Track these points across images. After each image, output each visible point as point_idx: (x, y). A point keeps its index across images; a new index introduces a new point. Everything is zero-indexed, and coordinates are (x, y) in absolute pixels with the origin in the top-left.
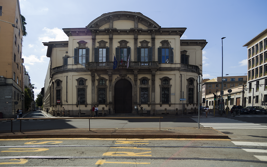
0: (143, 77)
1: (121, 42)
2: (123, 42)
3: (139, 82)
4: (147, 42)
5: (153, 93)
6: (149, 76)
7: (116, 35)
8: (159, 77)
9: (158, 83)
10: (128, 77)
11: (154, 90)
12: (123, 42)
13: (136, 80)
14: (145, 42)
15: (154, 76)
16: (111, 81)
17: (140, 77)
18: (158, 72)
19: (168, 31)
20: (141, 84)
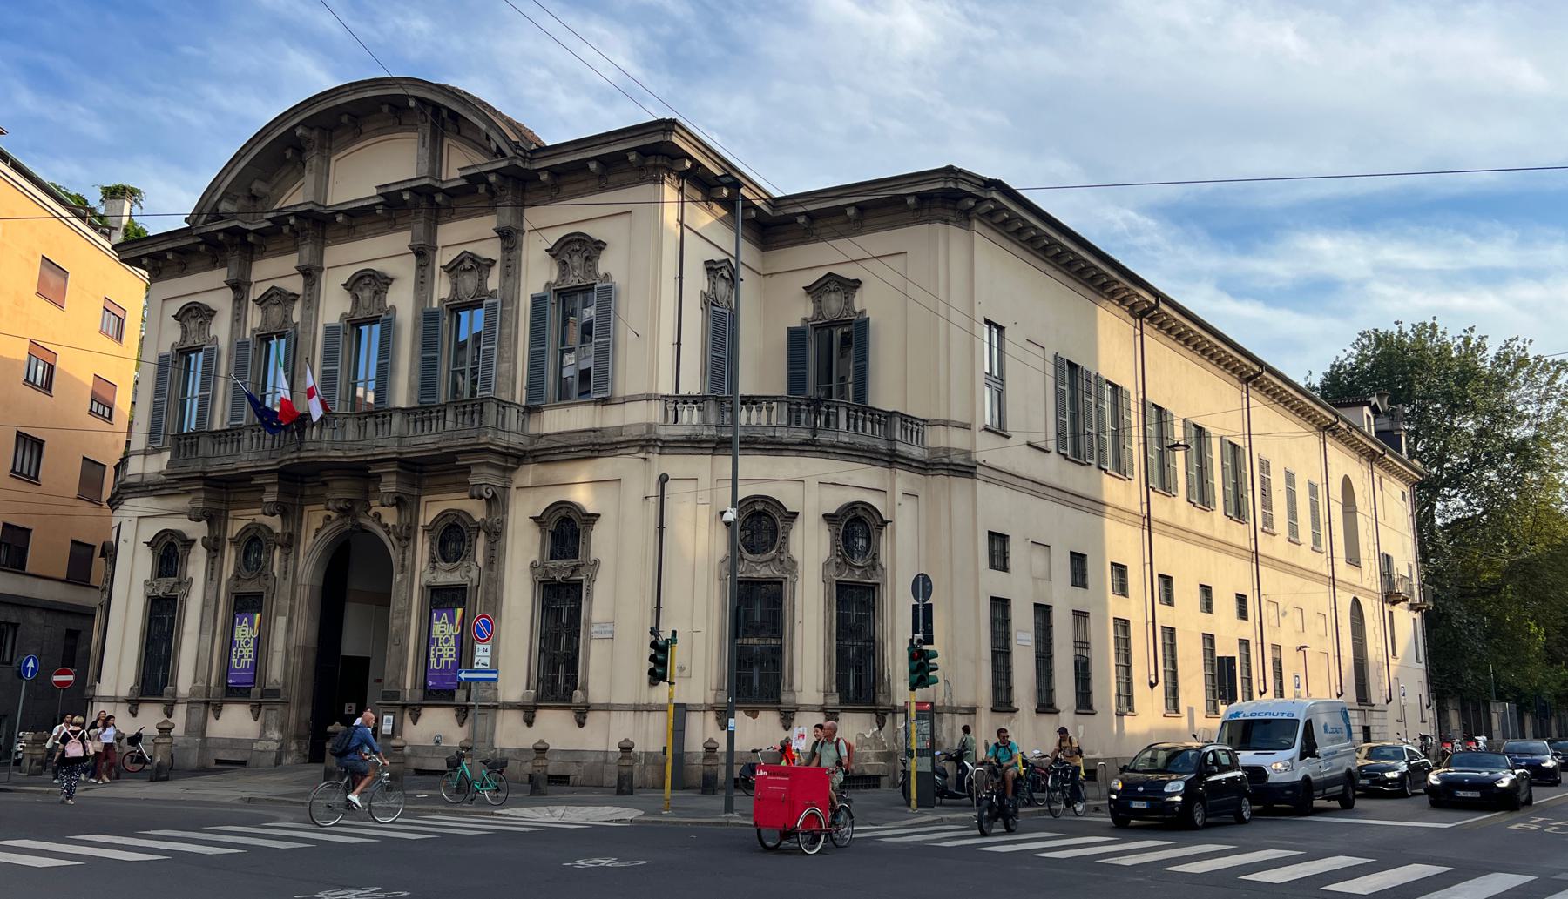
1: (353, 285)
3: (423, 546)
9: (523, 548)
17: (430, 511)
18: (528, 474)
19: (582, 166)
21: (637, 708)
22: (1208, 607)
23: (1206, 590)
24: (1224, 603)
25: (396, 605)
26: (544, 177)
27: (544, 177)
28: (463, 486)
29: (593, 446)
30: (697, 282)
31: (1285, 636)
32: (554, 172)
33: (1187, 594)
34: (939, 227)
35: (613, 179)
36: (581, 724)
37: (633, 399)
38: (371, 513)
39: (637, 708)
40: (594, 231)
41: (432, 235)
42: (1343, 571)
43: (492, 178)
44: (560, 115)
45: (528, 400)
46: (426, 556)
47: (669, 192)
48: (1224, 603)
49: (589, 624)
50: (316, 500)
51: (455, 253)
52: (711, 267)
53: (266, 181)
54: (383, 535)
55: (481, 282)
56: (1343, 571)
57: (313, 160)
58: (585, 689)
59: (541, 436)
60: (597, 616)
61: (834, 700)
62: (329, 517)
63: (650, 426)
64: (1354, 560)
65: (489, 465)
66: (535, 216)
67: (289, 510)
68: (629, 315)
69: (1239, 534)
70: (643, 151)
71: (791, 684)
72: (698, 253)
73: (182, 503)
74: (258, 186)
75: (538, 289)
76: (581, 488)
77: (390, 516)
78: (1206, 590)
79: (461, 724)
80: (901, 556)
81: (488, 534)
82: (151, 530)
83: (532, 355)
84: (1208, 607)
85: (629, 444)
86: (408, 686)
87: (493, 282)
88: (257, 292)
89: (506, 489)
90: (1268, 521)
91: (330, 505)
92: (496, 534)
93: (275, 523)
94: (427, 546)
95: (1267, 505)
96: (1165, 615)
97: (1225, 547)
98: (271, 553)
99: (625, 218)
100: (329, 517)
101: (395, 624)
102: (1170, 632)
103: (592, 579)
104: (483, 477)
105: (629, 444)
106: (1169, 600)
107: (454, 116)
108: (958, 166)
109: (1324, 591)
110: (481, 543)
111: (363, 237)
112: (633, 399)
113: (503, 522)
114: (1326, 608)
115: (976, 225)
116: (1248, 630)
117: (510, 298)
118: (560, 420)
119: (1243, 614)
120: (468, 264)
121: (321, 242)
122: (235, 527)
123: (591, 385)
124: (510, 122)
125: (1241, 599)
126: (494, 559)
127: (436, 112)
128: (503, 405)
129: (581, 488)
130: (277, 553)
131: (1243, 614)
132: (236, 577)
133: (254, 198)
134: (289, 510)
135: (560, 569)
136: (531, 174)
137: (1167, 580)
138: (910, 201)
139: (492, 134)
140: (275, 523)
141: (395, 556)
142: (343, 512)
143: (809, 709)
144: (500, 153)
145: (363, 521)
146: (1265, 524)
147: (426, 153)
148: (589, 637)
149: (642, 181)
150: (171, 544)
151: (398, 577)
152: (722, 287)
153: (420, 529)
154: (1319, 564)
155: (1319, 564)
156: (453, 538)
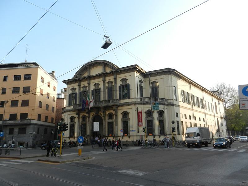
0: (109, 113)
1: (95, 85)
2: (97, 85)
3: (107, 117)
4: (112, 82)
5: (116, 127)
6: (114, 113)
7: (92, 80)
8: (120, 111)
9: (120, 117)
10: (100, 114)
11: (117, 125)
12: (97, 85)
13: (104, 116)
14: (110, 82)
15: (116, 112)
16: (89, 117)
17: (107, 112)
18: (120, 108)
19: (125, 70)
20: (108, 119)
22: (200, 120)
23: (200, 118)
24: (202, 120)
25: (104, 124)
26: (120, 71)
27: (120, 71)
28: (112, 109)
30: (139, 83)
31: (209, 123)
34: (167, 75)
35: (128, 71)
37: (133, 98)
41: (105, 79)
42: (216, 115)
43: (113, 72)
44: (121, 64)
47: (135, 73)
48: (202, 120)
51: (108, 81)
53: (82, 72)
54: (101, 116)
55: (112, 84)
56: (216, 115)
57: (88, 70)
59: (121, 103)
63: (135, 102)
64: (217, 113)
65: (115, 107)
66: (118, 76)
67: (89, 113)
68: (132, 87)
69: (203, 110)
70: (132, 68)
72: (139, 80)
73: (75, 113)
74: (81, 73)
75: (119, 85)
77: (102, 114)
78: (200, 118)
80: (166, 115)
81: (115, 115)
82: (70, 116)
83: (119, 93)
84: (200, 120)
85: (133, 104)
86: (106, 134)
87: (113, 84)
88: (82, 86)
90: (206, 109)
92: (116, 115)
93: (87, 115)
95: (206, 106)
96: (196, 122)
99: (130, 76)
101: (103, 127)
104: (115, 108)
105: (133, 104)
106: (196, 120)
107: (107, 64)
108: (170, 68)
109: (213, 117)
110: (114, 116)
111: (96, 79)
112: (133, 98)
113: (117, 114)
114: (214, 119)
115: (172, 75)
116: (205, 123)
117: (116, 86)
118: (123, 101)
119: (204, 121)
120: (110, 82)
121: (90, 80)
122: (81, 116)
123: (128, 96)
124: (115, 65)
125: (204, 119)
127: (105, 64)
128: (117, 99)
130: (87, 118)
131: (204, 121)
132: (82, 121)
133: (81, 74)
134: (89, 113)
135: (125, 119)
136: (117, 71)
137: (195, 117)
138: (164, 72)
139: (113, 67)
140: (87, 115)
141: (103, 118)
142: (96, 113)
144: (114, 69)
145: (98, 114)
147: (103, 68)
149: (132, 72)
150: (73, 118)
151: (104, 121)
154: (212, 114)
155: (212, 114)
156: (110, 116)
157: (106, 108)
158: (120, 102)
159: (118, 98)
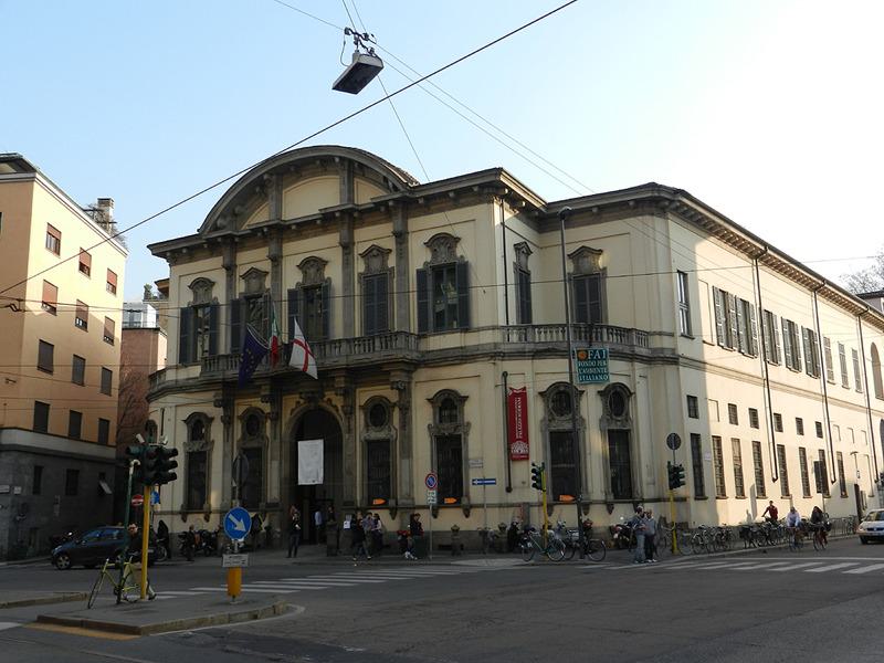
0: (372, 399)
3: (360, 417)
6: (393, 396)
9: (423, 417)
10: (330, 400)
13: (350, 412)
17: (363, 396)
18: (422, 374)
20: (367, 425)
21: (500, 506)
22: (801, 431)
24: (810, 428)
28: (386, 382)
29: (463, 356)
31: (843, 446)
32: (427, 198)
33: (789, 424)
36: (467, 516)
38: (325, 399)
39: (500, 506)
40: (456, 231)
44: (427, 165)
45: (419, 331)
46: (362, 422)
48: (810, 428)
49: (467, 459)
50: (290, 392)
52: (517, 247)
58: (468, 496)
60: (472, 455)
61: (611, 498)
62: (298, 402)
67: (275, 400)
69: (815, 385)
71: (587, 489)
76: (453, 378)
77: (338, 401)
78: (799, 421)
79: (393, 518)
84: (801, 431)
86: (358, 498)
89: (409, 383)
90: (831, 376)
91: (303, 396)
92: (406, 409)
93: (267, 408)
94: (362, 417)
95: (830, 366)
96: (780, 438)
97: (808, 394)
98: (264, 424)
100: (298, 402)
102: (782, 448)
103: (467, 434)
106: (780, 429)
109: (865, 416)
110: (396, 415)
114: (866, 427)
116: (823, 444)
117: (404, 272)
119: (820, 434)
122: (240, 410)
125: (818, 425)
126: (406, 422)
129: (453, 378)
131: (820, 434)
137: (778, 417)
141: (343, 423)
143: (597, 502)
145: (320, 403)
146: (829, 378)
148: (468, 467)
152: (523, 257)
153: (357, 407)
154: (860, 400)
157: (359, 374)
158: (423, 347)
159: (414, 328)
